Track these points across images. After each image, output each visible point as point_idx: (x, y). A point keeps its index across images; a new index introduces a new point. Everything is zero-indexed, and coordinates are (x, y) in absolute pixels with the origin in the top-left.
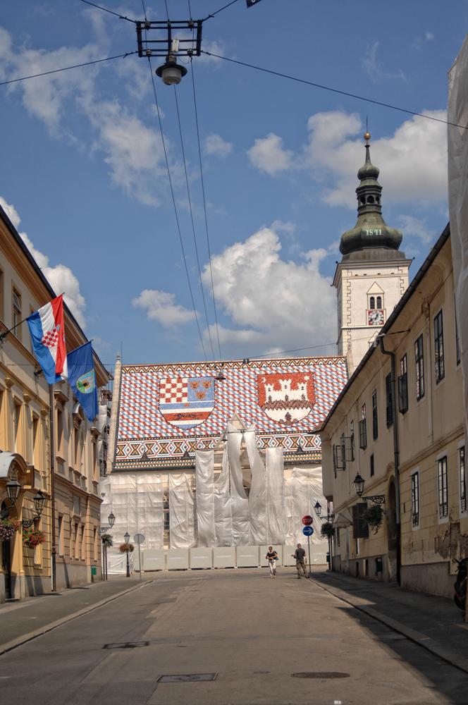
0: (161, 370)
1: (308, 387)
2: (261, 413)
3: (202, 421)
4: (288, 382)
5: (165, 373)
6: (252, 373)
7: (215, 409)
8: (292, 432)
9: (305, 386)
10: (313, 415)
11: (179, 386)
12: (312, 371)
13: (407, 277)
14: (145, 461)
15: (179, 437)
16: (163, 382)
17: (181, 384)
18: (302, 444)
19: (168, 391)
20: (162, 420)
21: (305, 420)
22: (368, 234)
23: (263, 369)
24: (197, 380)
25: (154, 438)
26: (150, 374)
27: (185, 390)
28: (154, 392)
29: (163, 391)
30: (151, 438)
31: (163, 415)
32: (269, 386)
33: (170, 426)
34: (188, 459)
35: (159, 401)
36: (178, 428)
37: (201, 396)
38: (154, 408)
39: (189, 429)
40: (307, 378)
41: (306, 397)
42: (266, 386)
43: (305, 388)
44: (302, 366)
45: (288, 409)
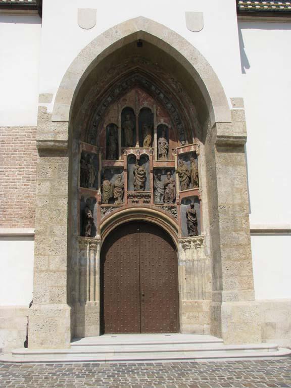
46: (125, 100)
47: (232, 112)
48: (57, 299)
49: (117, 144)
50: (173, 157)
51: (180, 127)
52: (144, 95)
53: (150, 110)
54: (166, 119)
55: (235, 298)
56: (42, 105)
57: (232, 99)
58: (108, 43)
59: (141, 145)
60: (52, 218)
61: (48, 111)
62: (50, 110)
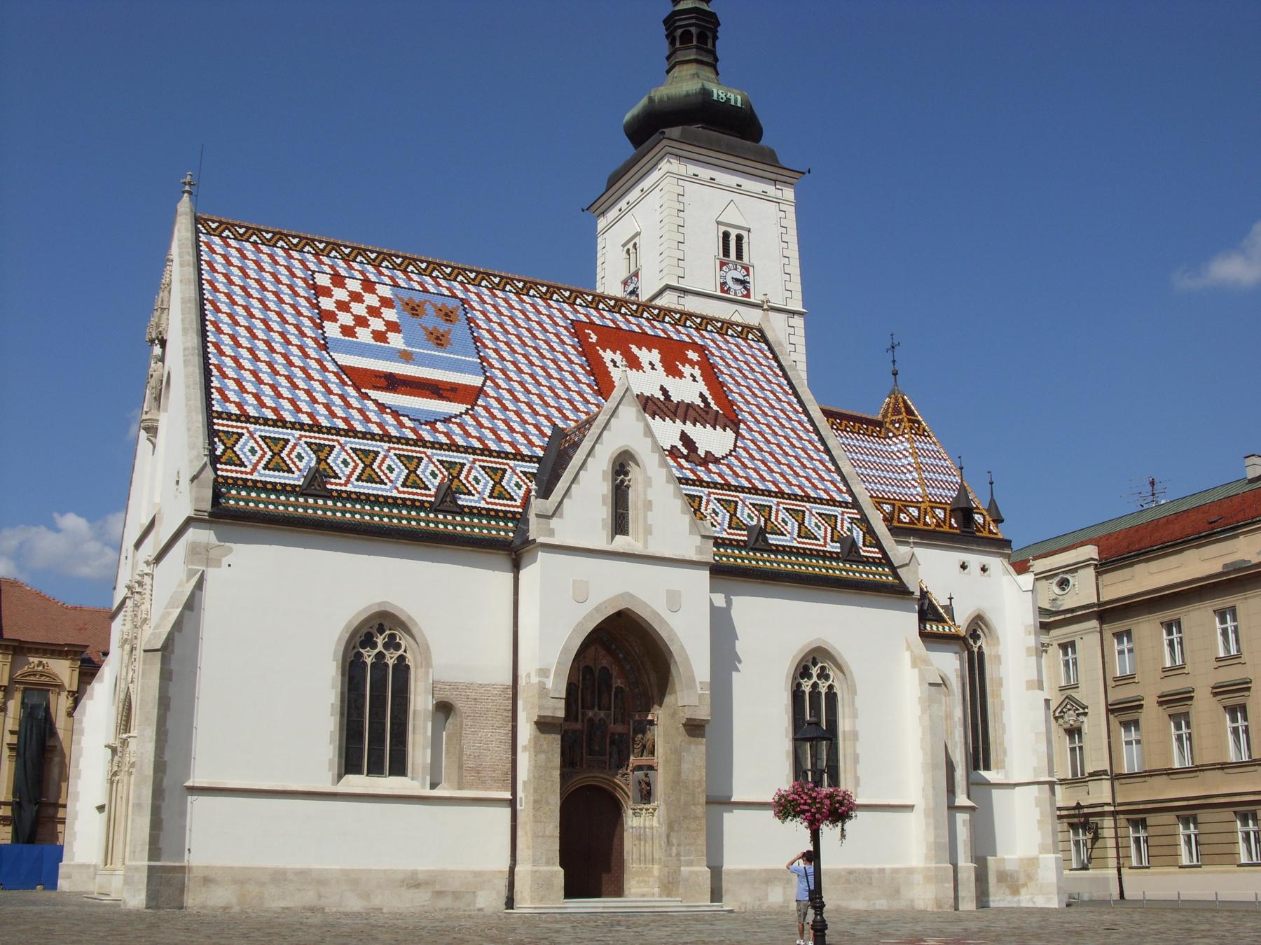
3: (461, 408)
4: (655, 356)
7: (489, 383)
8: (715, 485)
9: (697, 372)
10: (745, 449)
13: (792, 209)
15: (407, 441)
16: (323, 280)
19: (344, 307)
20: (345, 384)
21: (732, 459)
22: (715, 97)
24: (418, 298)
25: (329, 431)
27: (390, 314)
29: (327, 304)
31: (340, 367)
34: (454, 513)
35: (322, 328)
36: (396, 414)
37: (439, 340)
41: (710, 400)
42: (601, 352)
43: (699, 378)
45: (678, 421)
46: (584, 657)
47: (701, 696)
48: (551, 862)
49: (577, 705)
50: (629, 722)
51: (636, 691)
52: (603, 652)
53: (608, 671)
54: (623, 680)
55: (690, 863)
56: (542, 679)
57: (701, 683)
58: (599, 619)
59: (599, 709)
60: (546, 788)
61: (547, 687)
62: (550, 684)
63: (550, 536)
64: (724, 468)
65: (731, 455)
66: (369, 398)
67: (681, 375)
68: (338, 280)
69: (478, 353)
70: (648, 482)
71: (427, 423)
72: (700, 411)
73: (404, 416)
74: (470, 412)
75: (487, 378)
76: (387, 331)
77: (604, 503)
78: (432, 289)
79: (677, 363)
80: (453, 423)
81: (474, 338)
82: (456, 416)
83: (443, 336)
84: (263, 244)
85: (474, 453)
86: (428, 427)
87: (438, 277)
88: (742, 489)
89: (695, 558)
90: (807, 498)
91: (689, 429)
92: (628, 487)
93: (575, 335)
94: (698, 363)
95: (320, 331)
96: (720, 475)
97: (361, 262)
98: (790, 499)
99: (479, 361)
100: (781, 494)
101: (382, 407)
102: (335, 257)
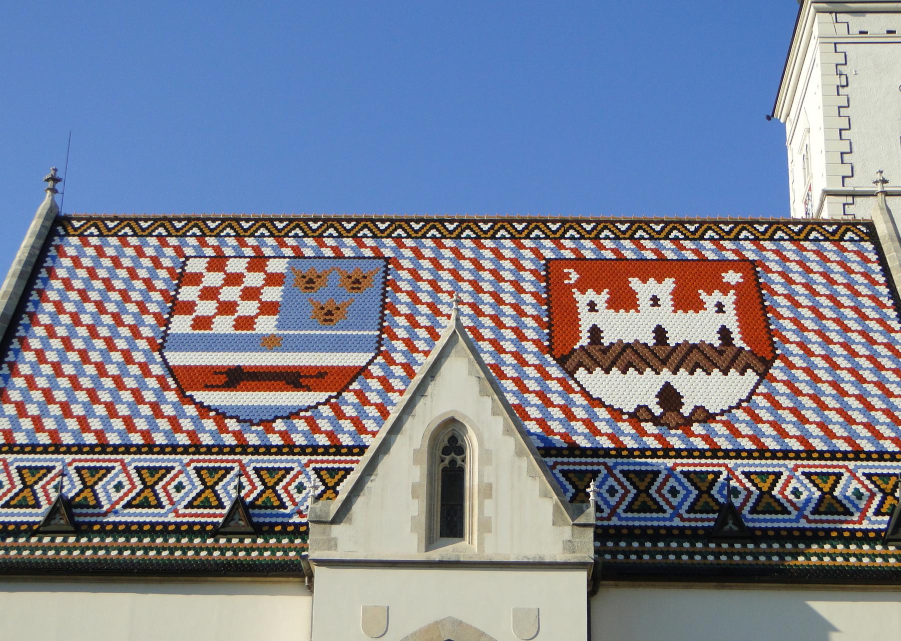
0: (196, 230)
1: (739, 305)
2: (560, 381)
3: (322, 396)
5: (212, 241)
6: (527, 254)
7: (380, 359)
8: (691, 453)
9: (729, 300)
10: (768, 397)
11: (254, 279)
12: (751, 256)
14: (54, 533)
15: (221, 449)
16: (195, 266)
17: (262, 276)
18: (737, 502)
19: (210, 293)
21: (740, 414)
23: (568, 243)
24: (319, 267)
25: (116, 449)
26: (153, 241)
27: (272, 294)
28: (156, 296)
29: (188, 293)
30: (103, 447)
31: (171, 371)
32: (591, 294)
33: (191, 410)
35: (167, 323)
36: (221, 415)
37: (328, 316)
38: (142, 344)
39: (267, 424)
40: (732, 277)
42: (577, 295)
44: (711, 239)
63: (329, 549)
64: (719, 428)
65: (738, 406)
66: (191, 400)
67: (699, 306)
68: (218, 262)
69: (381, 324)
70: (487, 457)
71: (261, 422)
72: (710, 353)
73: (231, 417)
74: (333, 401)
75: (379, 353)
76: (256, 316)
77: (414, 495)
78: (347, 252)
79: (700, 291)
80: (301, 418)
81: (384, 306)
82: (307, 409)
83: (338, 309)
84: (135, 234)
85: (315, 452)
86: (261, 428)
87: (365, 236)
88: (738, 453)
89: (560, 558)
90: (858, 454)
91: (682, 381)
92: (462, 470)
93: (547, 279)
94: (737, 287)
95: (164, 328)
96: (706, 438)
97: (263, 235)
98: (820, 459)
99: (378, 333)
100: (810, 453)
101: (204, 410)
102: (228, 235)
